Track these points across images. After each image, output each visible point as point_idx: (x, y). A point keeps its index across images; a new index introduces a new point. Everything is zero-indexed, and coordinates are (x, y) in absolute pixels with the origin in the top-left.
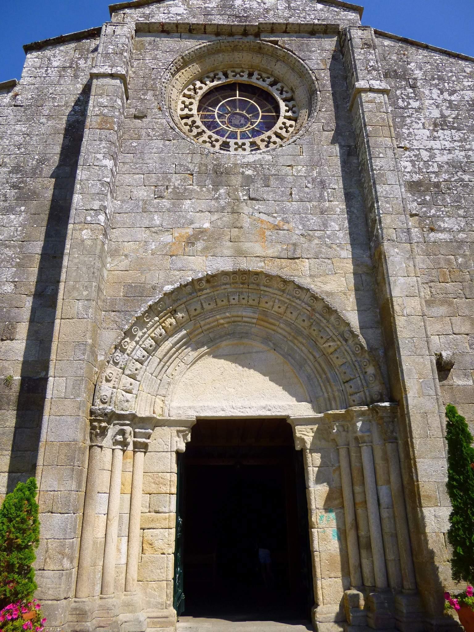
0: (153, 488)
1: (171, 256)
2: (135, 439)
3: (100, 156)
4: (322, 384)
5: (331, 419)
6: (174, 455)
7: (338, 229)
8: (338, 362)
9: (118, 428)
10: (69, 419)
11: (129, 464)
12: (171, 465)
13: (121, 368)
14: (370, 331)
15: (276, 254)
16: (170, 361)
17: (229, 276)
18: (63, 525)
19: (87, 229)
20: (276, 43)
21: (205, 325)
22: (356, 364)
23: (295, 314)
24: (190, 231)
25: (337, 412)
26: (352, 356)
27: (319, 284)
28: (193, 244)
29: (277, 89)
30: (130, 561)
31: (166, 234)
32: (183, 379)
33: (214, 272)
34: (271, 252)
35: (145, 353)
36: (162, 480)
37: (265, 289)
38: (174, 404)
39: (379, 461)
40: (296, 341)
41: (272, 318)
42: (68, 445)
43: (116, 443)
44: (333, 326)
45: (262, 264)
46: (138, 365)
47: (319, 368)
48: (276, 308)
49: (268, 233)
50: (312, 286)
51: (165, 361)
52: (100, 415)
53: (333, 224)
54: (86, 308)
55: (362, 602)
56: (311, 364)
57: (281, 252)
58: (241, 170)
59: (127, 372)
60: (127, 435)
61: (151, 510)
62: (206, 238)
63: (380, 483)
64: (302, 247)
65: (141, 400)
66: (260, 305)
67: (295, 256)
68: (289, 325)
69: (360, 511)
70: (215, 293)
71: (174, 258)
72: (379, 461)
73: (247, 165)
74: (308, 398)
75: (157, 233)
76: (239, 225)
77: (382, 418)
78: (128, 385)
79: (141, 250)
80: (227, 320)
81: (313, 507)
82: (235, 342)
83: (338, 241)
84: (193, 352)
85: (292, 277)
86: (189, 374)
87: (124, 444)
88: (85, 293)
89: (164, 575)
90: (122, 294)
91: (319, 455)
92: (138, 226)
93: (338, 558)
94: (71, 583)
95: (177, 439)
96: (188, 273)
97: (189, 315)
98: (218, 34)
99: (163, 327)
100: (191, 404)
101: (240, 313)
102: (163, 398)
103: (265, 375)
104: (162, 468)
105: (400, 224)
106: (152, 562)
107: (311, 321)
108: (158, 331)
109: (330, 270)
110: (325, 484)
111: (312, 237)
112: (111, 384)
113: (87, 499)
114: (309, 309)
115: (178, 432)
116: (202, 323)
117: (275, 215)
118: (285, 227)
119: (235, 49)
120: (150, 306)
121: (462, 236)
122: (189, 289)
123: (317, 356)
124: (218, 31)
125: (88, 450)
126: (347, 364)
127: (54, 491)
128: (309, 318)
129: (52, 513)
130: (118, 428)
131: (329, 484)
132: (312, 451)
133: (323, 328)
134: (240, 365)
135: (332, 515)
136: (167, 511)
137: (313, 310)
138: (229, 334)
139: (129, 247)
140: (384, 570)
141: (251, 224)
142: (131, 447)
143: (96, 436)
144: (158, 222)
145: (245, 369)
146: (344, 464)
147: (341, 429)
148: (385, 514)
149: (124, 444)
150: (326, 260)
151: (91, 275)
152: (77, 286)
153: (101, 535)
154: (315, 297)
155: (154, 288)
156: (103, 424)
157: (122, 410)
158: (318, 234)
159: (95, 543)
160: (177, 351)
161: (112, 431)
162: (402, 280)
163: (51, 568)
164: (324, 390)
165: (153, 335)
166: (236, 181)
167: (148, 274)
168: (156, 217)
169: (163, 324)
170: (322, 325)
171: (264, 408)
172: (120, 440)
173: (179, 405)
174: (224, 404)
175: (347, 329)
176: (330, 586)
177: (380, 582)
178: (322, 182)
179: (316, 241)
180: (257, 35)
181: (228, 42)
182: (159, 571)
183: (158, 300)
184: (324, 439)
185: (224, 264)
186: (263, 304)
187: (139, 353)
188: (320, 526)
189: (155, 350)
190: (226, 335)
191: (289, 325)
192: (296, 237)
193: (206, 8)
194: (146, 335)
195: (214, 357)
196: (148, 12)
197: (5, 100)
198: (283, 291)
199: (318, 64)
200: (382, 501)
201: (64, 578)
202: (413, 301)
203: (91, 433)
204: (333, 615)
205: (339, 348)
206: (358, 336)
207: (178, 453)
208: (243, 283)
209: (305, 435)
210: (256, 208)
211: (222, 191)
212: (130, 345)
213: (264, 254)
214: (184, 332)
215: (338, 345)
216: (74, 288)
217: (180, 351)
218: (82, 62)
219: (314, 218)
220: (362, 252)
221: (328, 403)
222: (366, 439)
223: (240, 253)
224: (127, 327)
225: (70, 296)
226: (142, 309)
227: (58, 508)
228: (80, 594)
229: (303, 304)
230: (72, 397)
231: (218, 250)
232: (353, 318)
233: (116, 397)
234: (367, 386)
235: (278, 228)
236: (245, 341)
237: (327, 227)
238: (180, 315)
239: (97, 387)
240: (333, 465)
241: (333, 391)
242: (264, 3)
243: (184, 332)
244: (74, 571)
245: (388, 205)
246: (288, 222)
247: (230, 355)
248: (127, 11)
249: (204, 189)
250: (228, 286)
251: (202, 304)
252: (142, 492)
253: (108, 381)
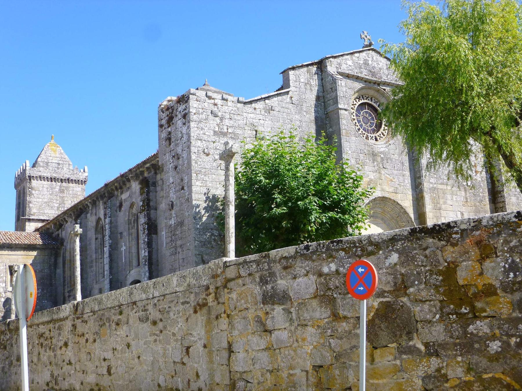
3: (348, 149)
20: (384, 90)
73: (381, 153)
98: (365, 81)
119: (370, 88)
121: (435, 186)
124: (366, 81)
154: (402, 208)
162: (428, 206)
166: (379, 159)
178: (403, 163)
180: (379, 85)
191: (391, 215)
218: (311, 81)
223: (383, 190)
232: (412, 216)
236: (377, 220)
248: (331, 59)
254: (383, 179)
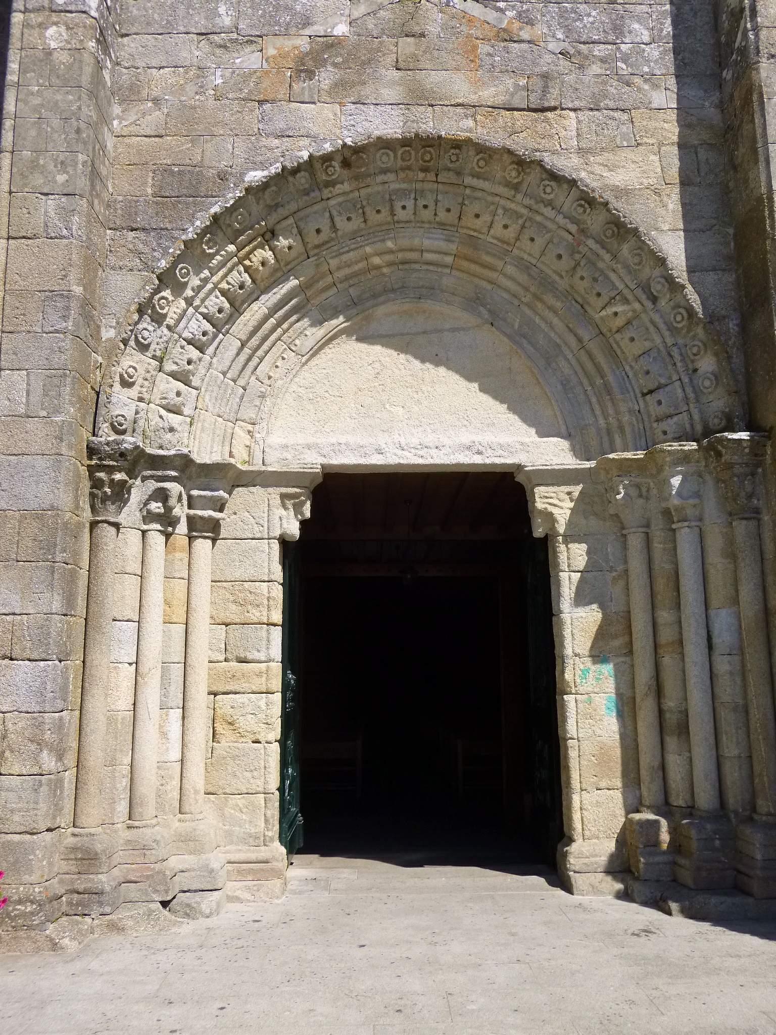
0: (233, 613)
1: (261, 102)
2: (192, 512)
4: (594, 400)
5: (615, 472)
6: (276, 546)
7: (646, 38)
8: (632, 350)
9: (153, 485)
10: (41, 463)
11: (180, 563)
12: (271, 565)
13: (154, 357)
14: (711, 277)
15: (500, 100)
16: (265, 347)
17: (394, 151)
18: (37, 684)
19: (56, 24)
21: (339, 268)
22: (675, 352)
23: (540, 242)
24: (302, 43)
25: (629, 455)
26: (667, 333)
27: (598, 170)
28: (310, 74)
30: (189, 755)
31: (249, 49)
32: (294, 387)
33: (361, 140)
34: (489, 94)
35: (208, 327)
36: (251, 597)
37: (475, 182)
38: (276, 439)
39: (716, 559)
40: (539, 305)
41: (488, 253)
42: (39, 518)
43: (149, 517)
44: (627, 267)
45: (470, 123)
46: (194, 353)
47: (589, 366)
48: (498, 230)
49: (484, 48)
50: (583, 175)
51: (254, 346)
52: (111, 457)
53: (636, 26)
54: (66, 214)
55: (665, 837)
56: (570, 356)
57: (512, 95)
59: (169, 367)
60: (173, 501)
61: (230, 656)
62: (340, 59)
63: (714, 602)
64: (563, 82)
65: (203, 430)
66: (463, 223)
67: (546, 104)
68: (525, 267)
69: (667, 661)
70: (363, 192)
71: (267, 106)
72: (716, 559)
74: (563, 428)
75: (225, 47)
76: (417, 29)
77: (730, 466)
78: (172, 395)
79: (191, 89)
80: (388, 258)
81: (568, 651)
82: (406, 307)
83: (646, 69)
84: (314, 330)
85: (538, 154)
86: (305, 373)
87: (168, 521)
88: (61, 178)
89: (260, 782)
90: (149, 191)
91: (584, 546)
92: (182, 29)
93: (618, 752)
94: (61, 798)
95: (282, 512)
96: (301, 143)
97: (305, 244)
99: (247, 269)
100: (311, 440)
101: (416, 242)
102: (250, 427)
103: (469, 378)
104: (251, 573)
106: (234, 758)
107: (577, 256)
108: (235, 277)
109: (624, 137)
110: (595, 606)
111: (586, 57)
112: (134, 392)
113: (91, 633)
114: (573, 228)
115: (283, 497)
116: (334, 263)
118: (525, 35)
120: (216, 218)
122: (303, 181)
123: (586, 338)
125: (87, 530)
126: (653, 354)
127: (14, 614)
128: (573, 251)
129: (12, 659)
130: (153, 485)
131: (602, 607)
132: (569, 538)
133: (602, 272)
134: (416, 357)
135: (608, 669)
136: (263, 659)
137: (582, 231)
138: (393, 290)
139: (161, 80)
140: (714, 776)
141: (445, 27)
142: (182, 528)
143: (103, 501)
144: (227, 21)
145: (428, 365)
146: (637, 565)
147: (634, 492)
148: (723, 666)
149: (168, 521)
150: (617, 114)
151: (73, 135)
152: (41, 162)
153: (123, 702)
154: (588, 201)
155: (223, 177)
156: (118, 476)
157: (161, 447)
158: (599, 51)
159: (111, 721)
160: (279, 324)
161: (139, 491)
163: (16, 769)
164: (598, 412)
165: (224, 285)
167: (209, 145)
168: (222, 10)
169: (247, 262)
170: (601, 265)
171: (469, 448)
172: (157, 510)
173: (284, 442)
174: (382, 440)
175: (657, 272)
176: (598, 804)
177: (705, 798)
179: (596, 69)
182: (248, 775)
183: (232, 202)
184: (596, 514)
185: (383, 122)
186: (469, 221)
187: (193, 324)
188: (581, 689)
189: (231, 319)
190: (385, 291)
191: (525, 267)
192: (548, 58)
194: (210, 286)
195: (359, 340)
198: (516, 187)
200: (716, 640)
201: (44, 789)
203: (92, 496)
204: (603, 860)
205: (637, 317)
206: (683, 287)
207: (285, 543)
208: (425, 170)
209: (555, 505)
212: (174, 308)
213: (473, 99)
214: (293, 283)
215: (634, 311)
216: (34, 166)
217: (285, 326)
219: (594, 13)
220: (701, 93)
221: (606, 439)
222: (689, 512)
223: (419, 97)
224: (163, 264)
225: (25, 185)
226: (198, 223)
227: (24, 649)
228: (83, 820)
229: (560, 219)
230: (44, 413)
231: (367, 90)
232: (674, 248)
233: (147, 420)
234: (697, 400)
235: (507, 37)
236: (427, 304)
237: (622, 33)
238: (283, 242)
239: (103, 397)
240: (612, 569)
241: (617, 412)
243: (293, 283)
244: (69, 777)
246: (531, 23)
247: (393, 336)
250: (391, 177)
251: (332, 218)
252: (209, 621)
253: (126, 384)
254: (433, 29)
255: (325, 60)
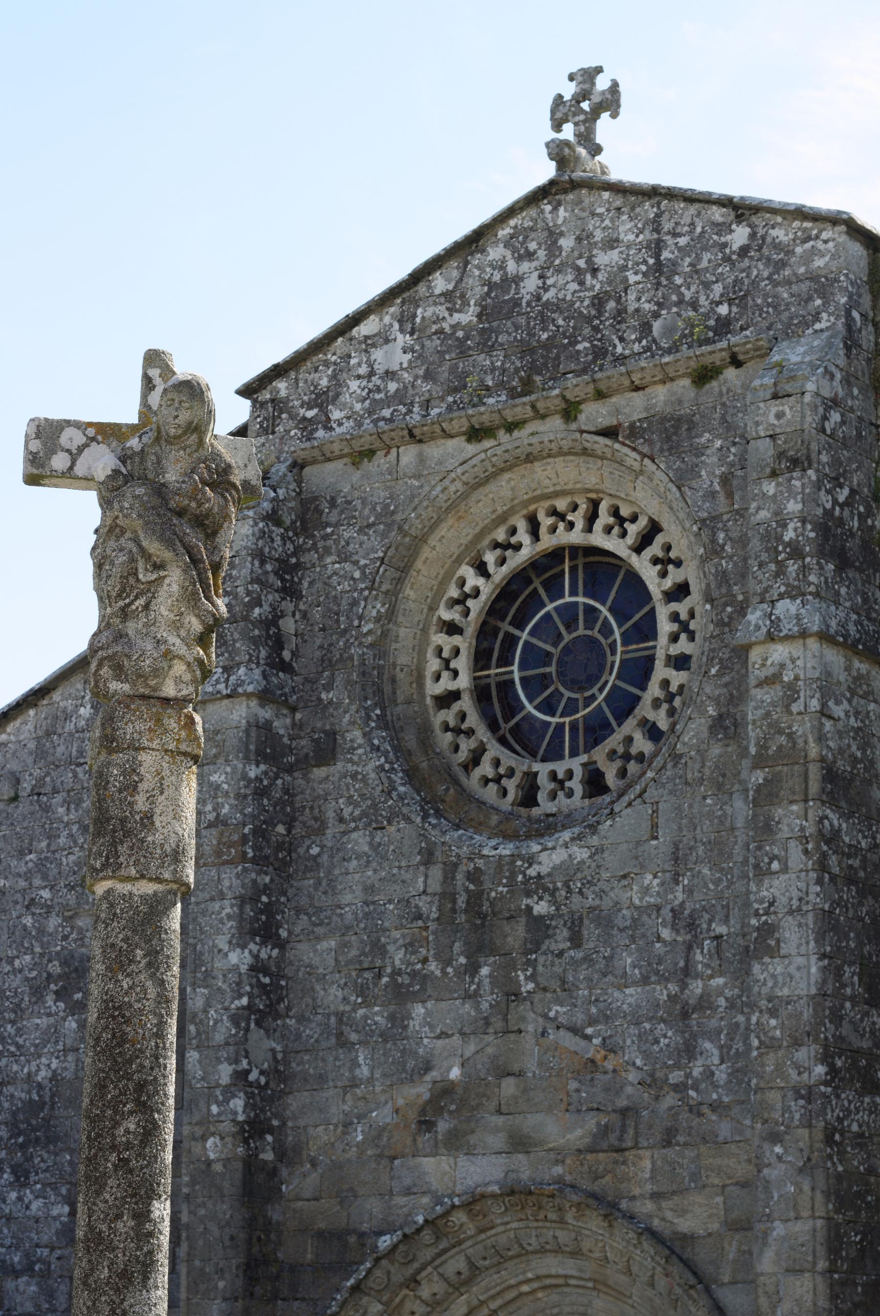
27: (669, 1215)
29: (655, 561)
58: (526, 901)
76: (516, 1068)
105: (793, 1073)
117: (589, 1031)
181: (507, 451)
193: (455, 327)
196: (324, 382)
197: (82, 711)
199: (713, 494)
202: (798, 1283)
210: (552, 1014)
211: (485, 971)
219: (670, 1034)
223: (519, 1143)
242: (595, 271)
245: (773, 1022)
249: (449, 970)
254: (531, 1066)
255: (442, 1108)
